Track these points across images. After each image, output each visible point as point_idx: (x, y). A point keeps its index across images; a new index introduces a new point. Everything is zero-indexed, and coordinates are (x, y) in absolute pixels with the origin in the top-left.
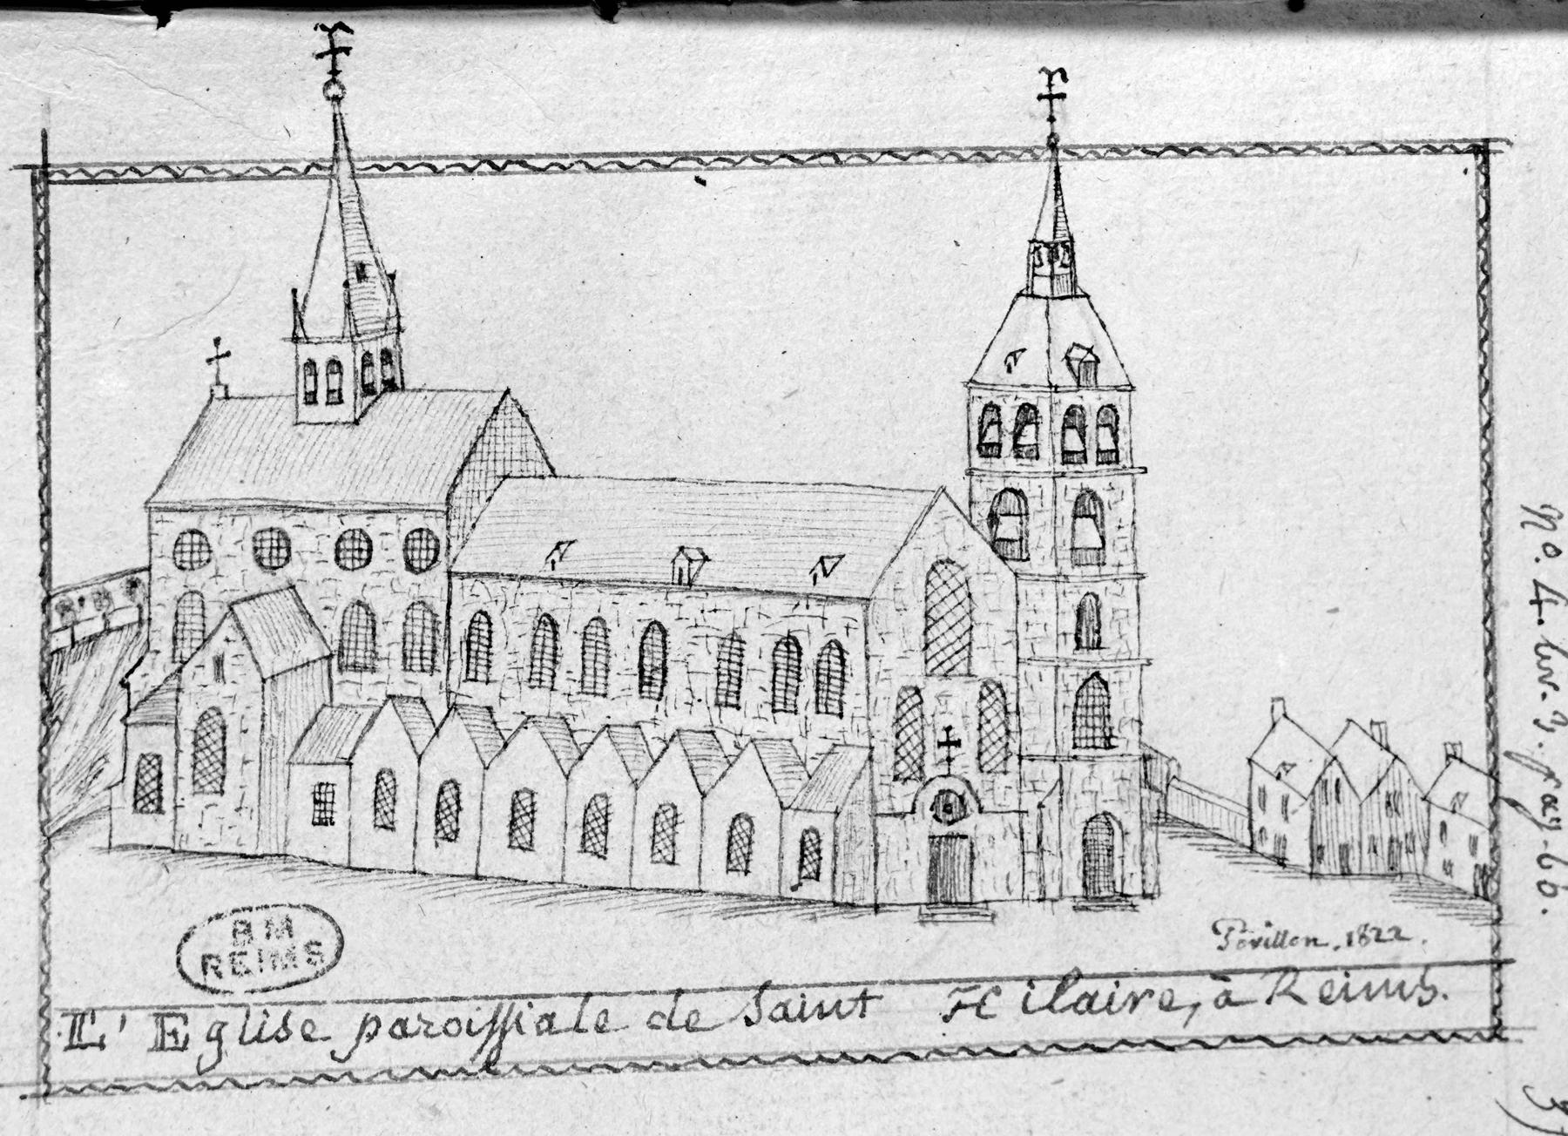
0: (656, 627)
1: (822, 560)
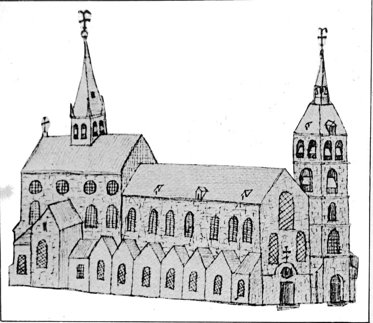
0: (190, 213)
1: (245, 191)
